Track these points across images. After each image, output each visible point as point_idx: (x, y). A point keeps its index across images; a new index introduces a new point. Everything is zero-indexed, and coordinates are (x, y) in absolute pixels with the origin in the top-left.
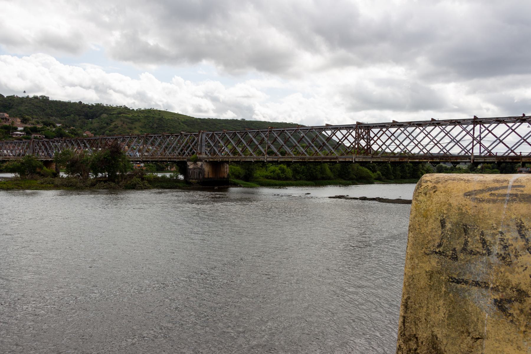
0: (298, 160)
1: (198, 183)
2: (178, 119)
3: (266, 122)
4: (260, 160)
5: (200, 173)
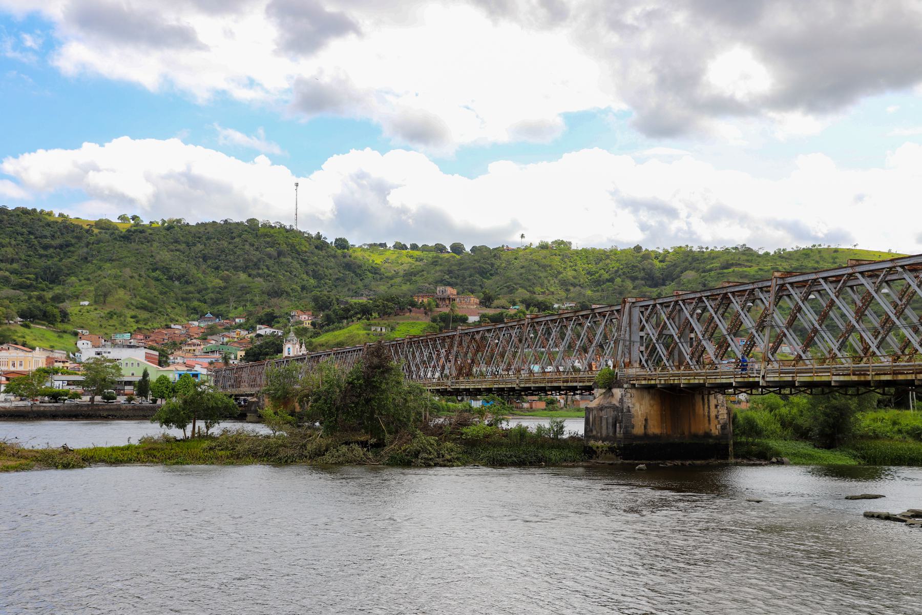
1: (611, 450)
4: (751, 380)
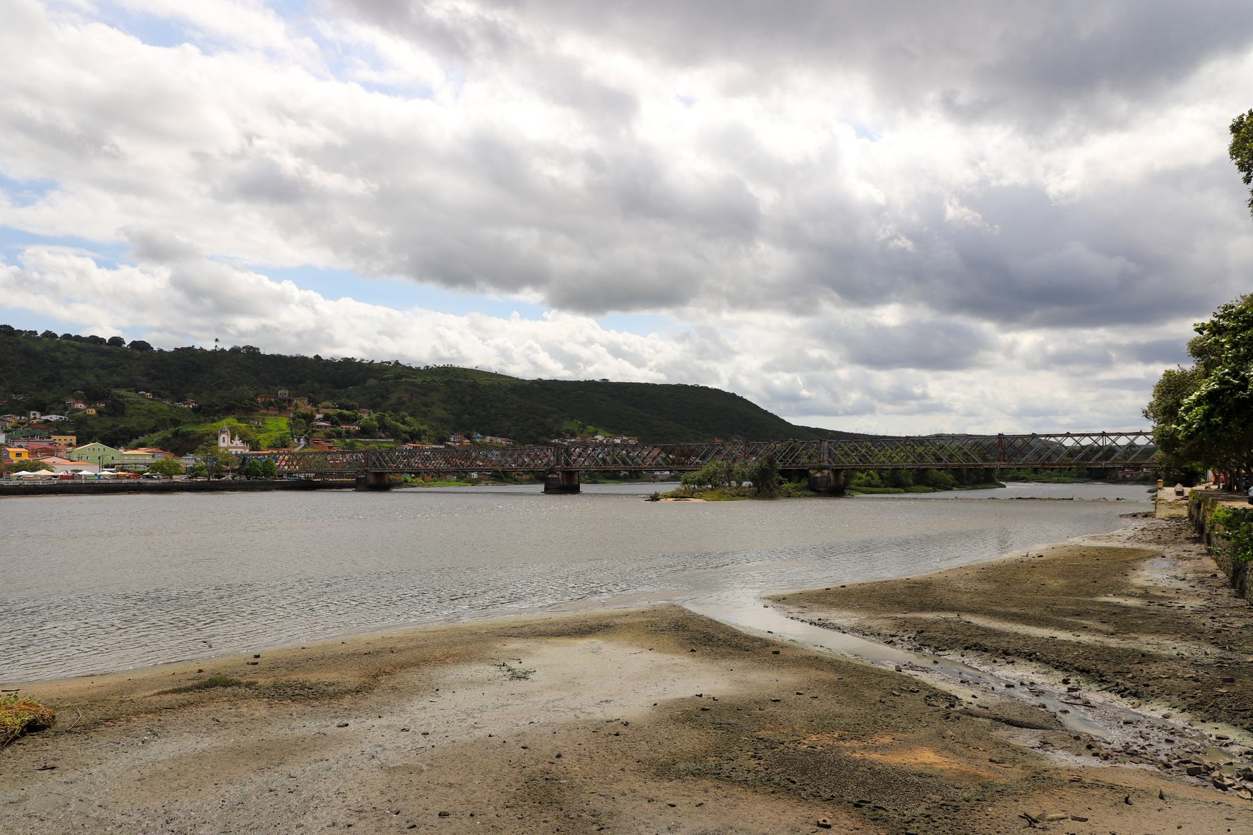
1: (826, 491)
2: (499, 384)
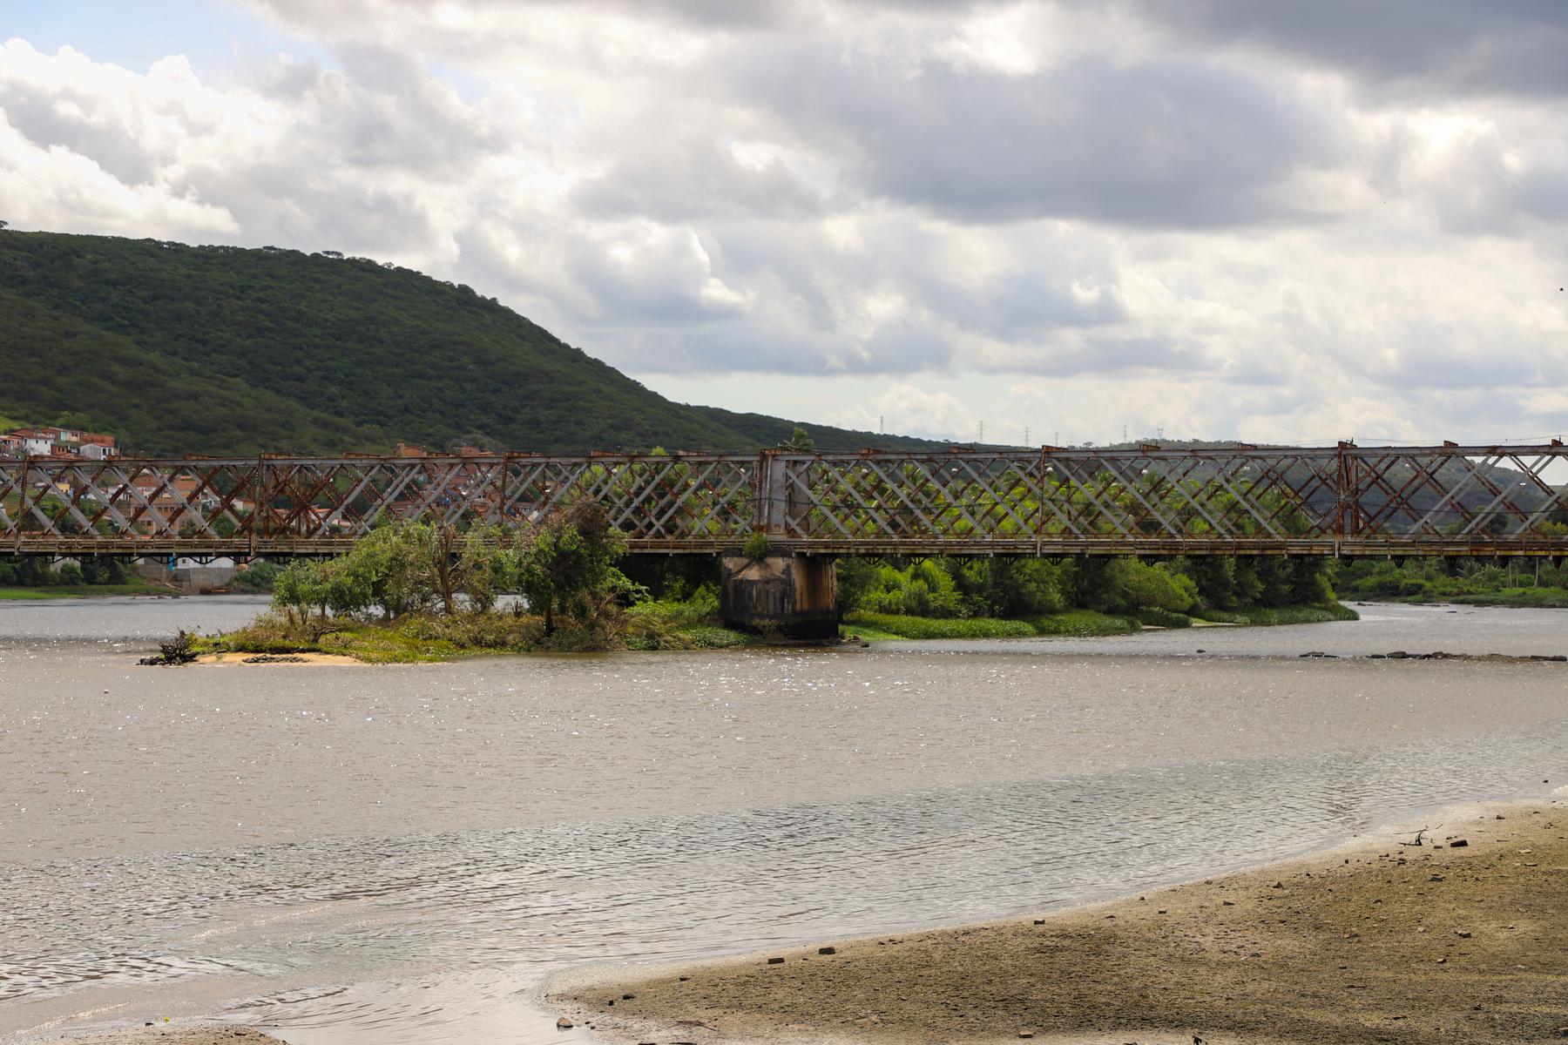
0: (1154, 552)
1: (779, 629)
3: (158, 244)
4: (1019, 551)
5: (784, 595)
